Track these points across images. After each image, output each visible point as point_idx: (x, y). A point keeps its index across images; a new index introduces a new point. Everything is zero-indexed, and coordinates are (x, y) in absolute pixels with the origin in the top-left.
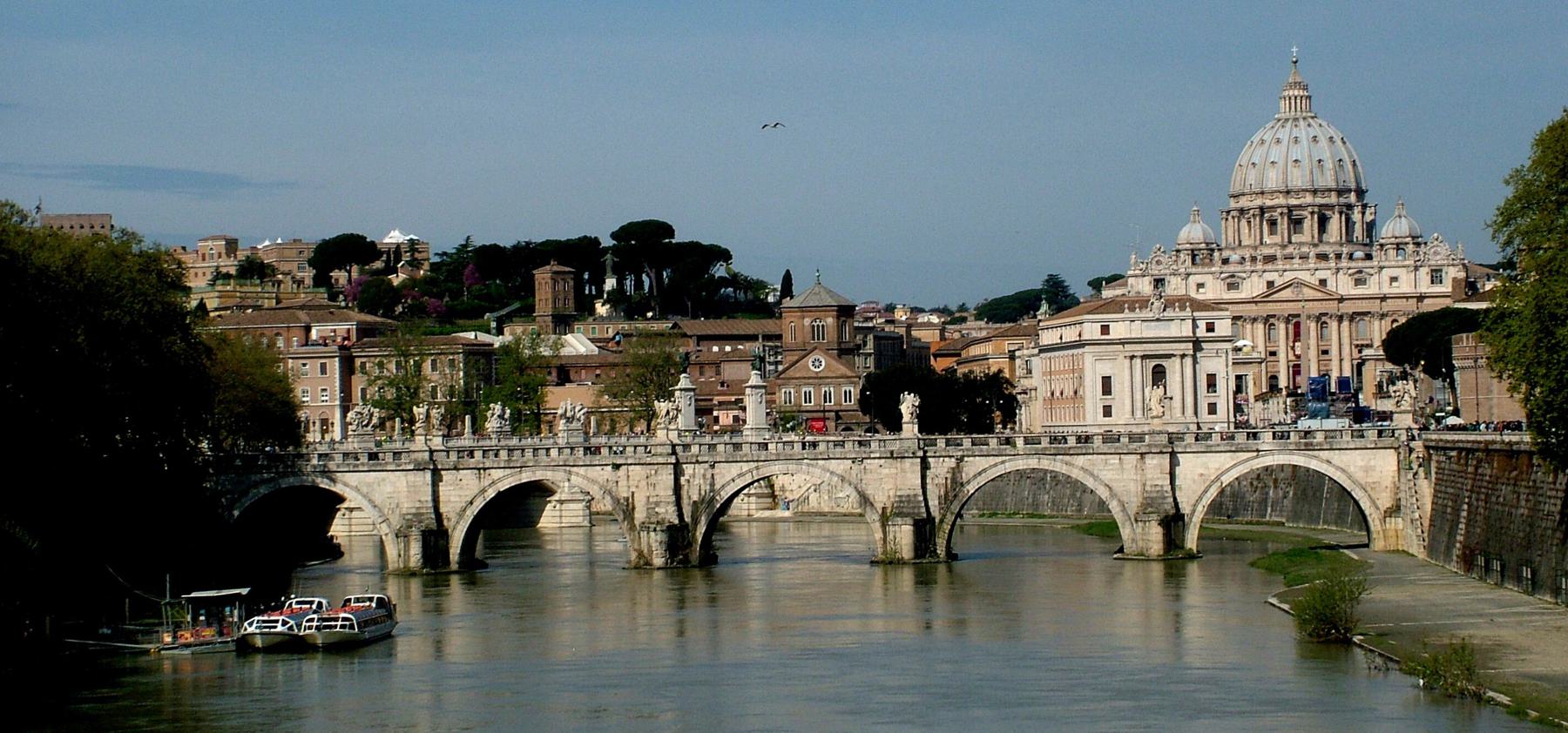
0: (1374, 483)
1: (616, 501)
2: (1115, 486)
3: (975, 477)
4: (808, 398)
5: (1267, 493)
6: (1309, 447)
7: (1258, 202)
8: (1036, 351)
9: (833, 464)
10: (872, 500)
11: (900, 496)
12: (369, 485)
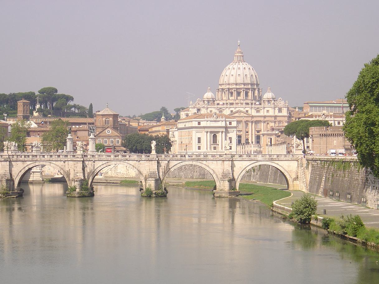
0: (291, 170)
1: (64, 171)
3: (173, 166)
5: (251, 173)
7: (228, 87)
8: (177, 129)
11: (151, 172)
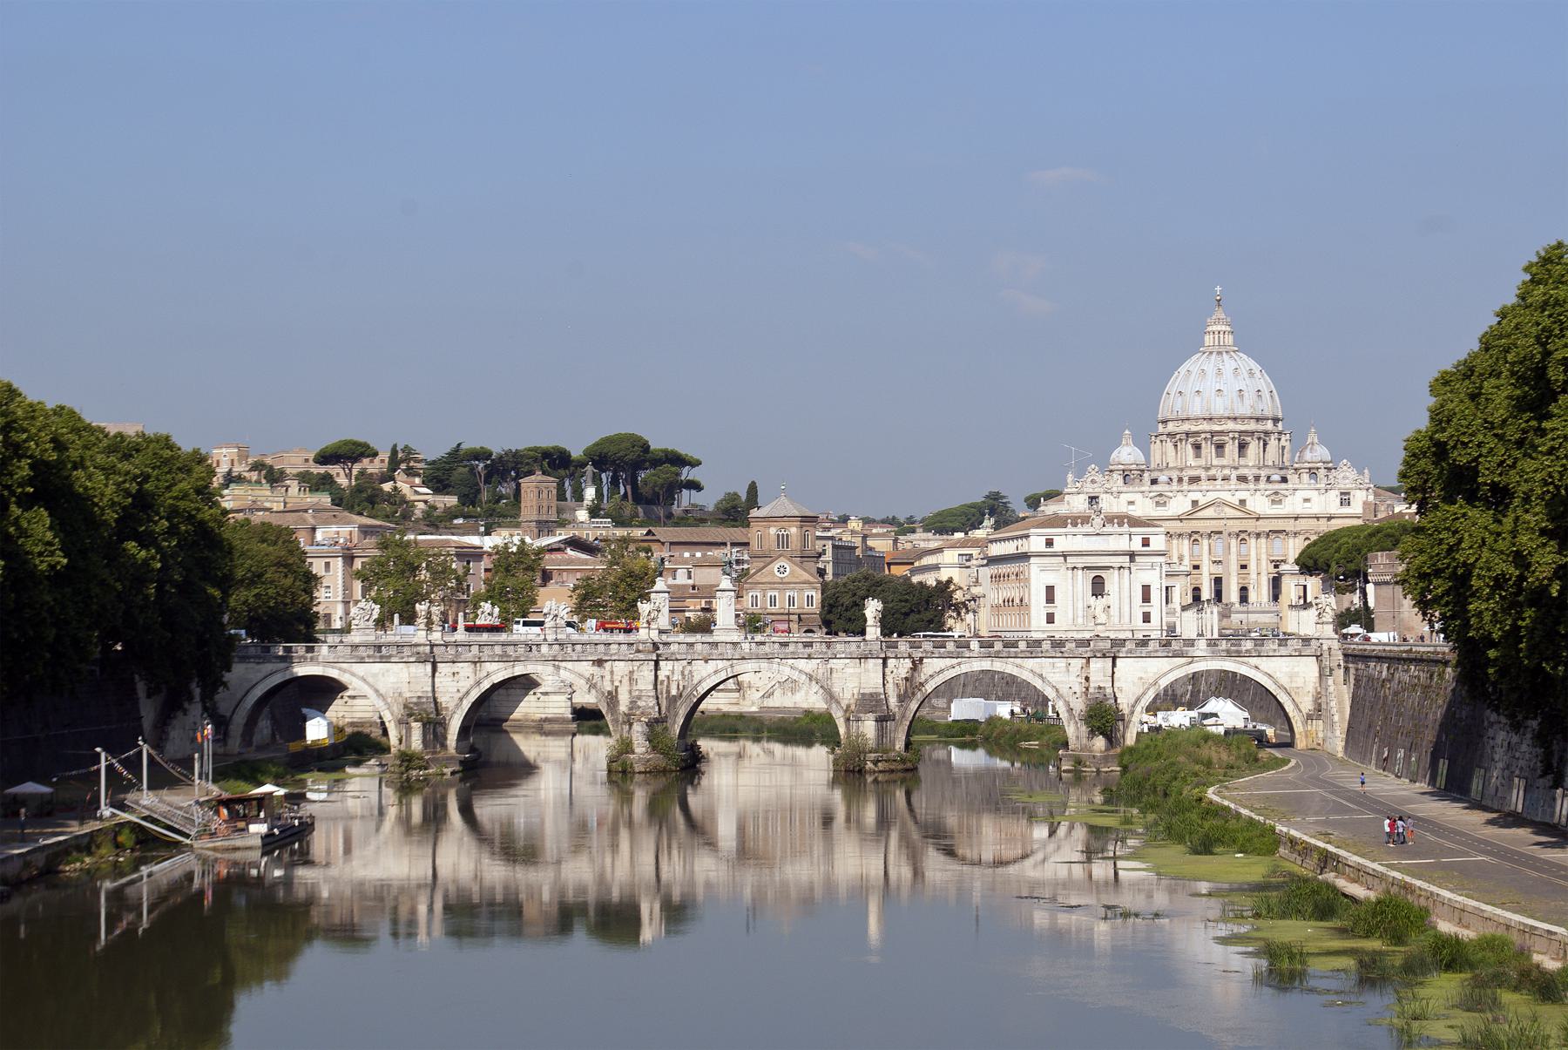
0: (1298, 688)
2: (1064, 690)
4: (773, 601)
7: (1186, 427)
8: (985, 562)
9: (802, 664)
12: (375, 675)
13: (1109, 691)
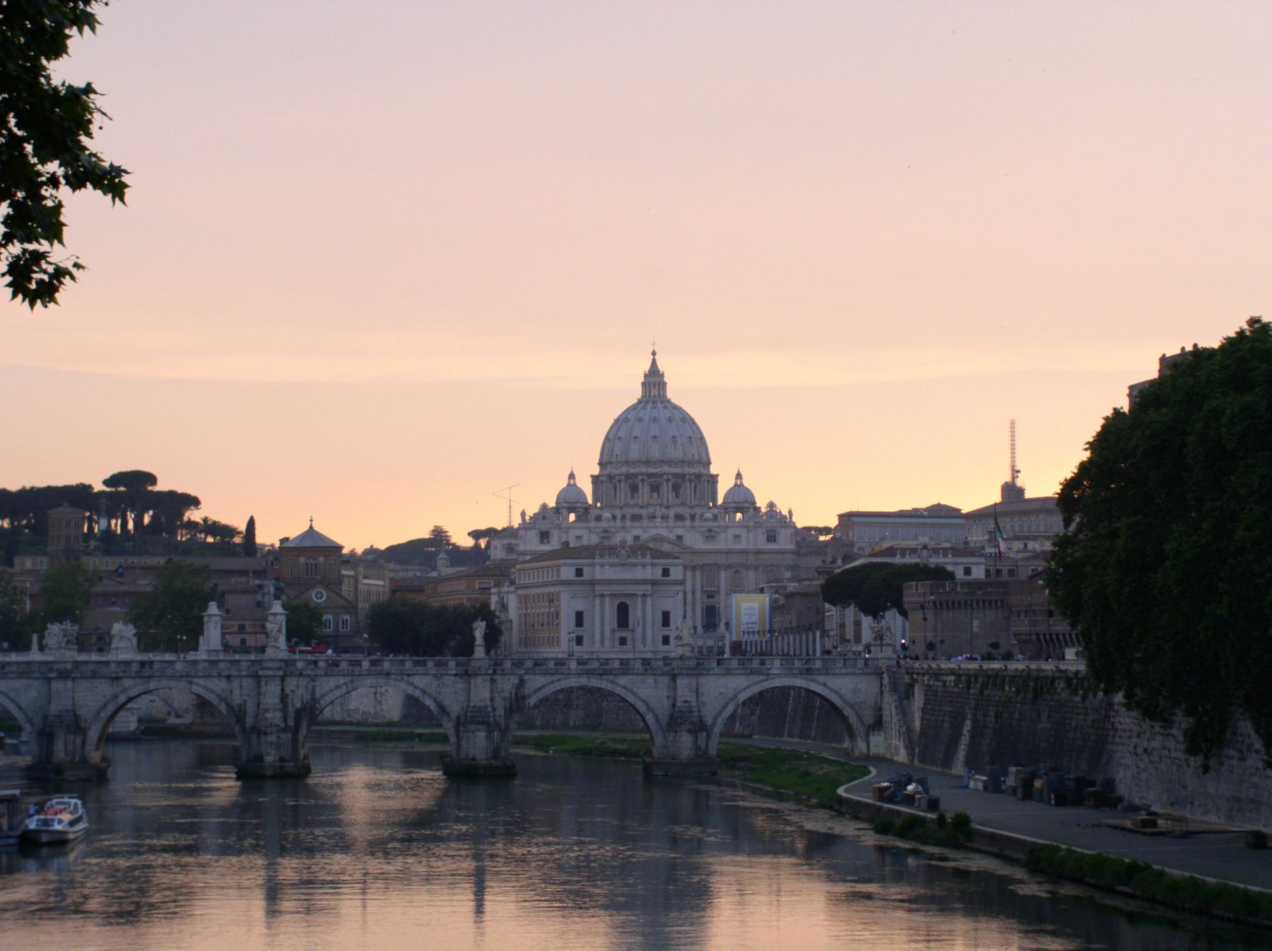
0: (860, 702)
1: (230, 707)
3: (535, 692)
6: (809, 671)
7: (624, 470)
8: (512, 589)
10: (448, 710)
13: (694, 704)
